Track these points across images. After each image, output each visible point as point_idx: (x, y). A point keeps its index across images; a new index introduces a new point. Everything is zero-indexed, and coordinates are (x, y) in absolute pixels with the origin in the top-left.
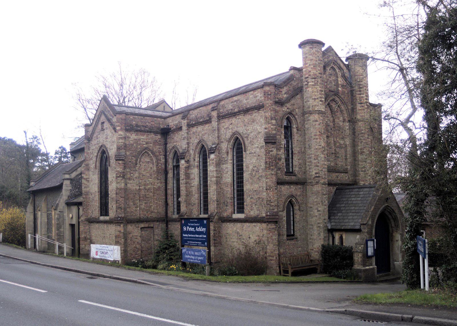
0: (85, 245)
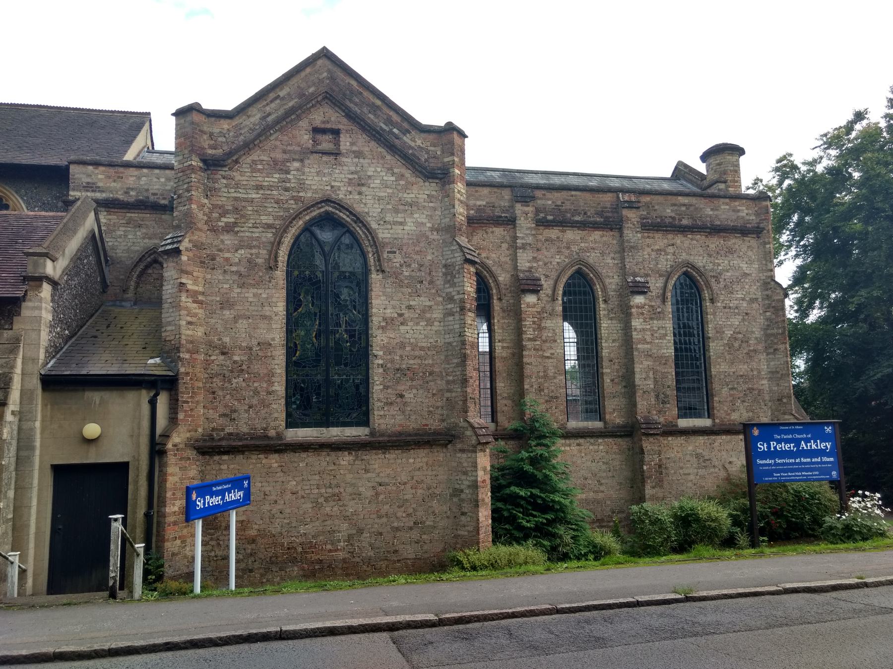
0: (183, 542)
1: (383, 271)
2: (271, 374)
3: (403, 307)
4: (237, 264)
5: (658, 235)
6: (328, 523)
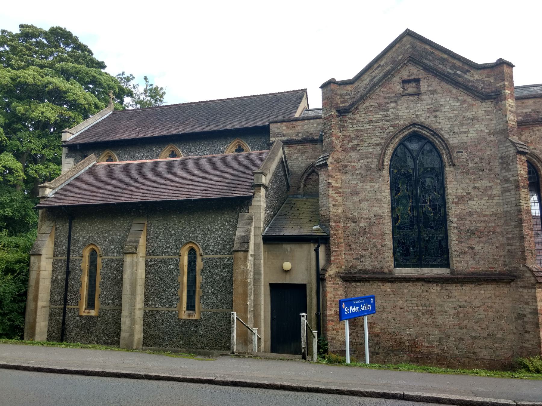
0: (337, 332)
1: (454, 165)
2: (383, 234)
3: (470, 188)
4: (360, 169)
6: (425, 329)
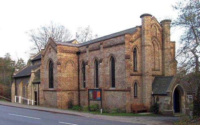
5: (107, 49)
